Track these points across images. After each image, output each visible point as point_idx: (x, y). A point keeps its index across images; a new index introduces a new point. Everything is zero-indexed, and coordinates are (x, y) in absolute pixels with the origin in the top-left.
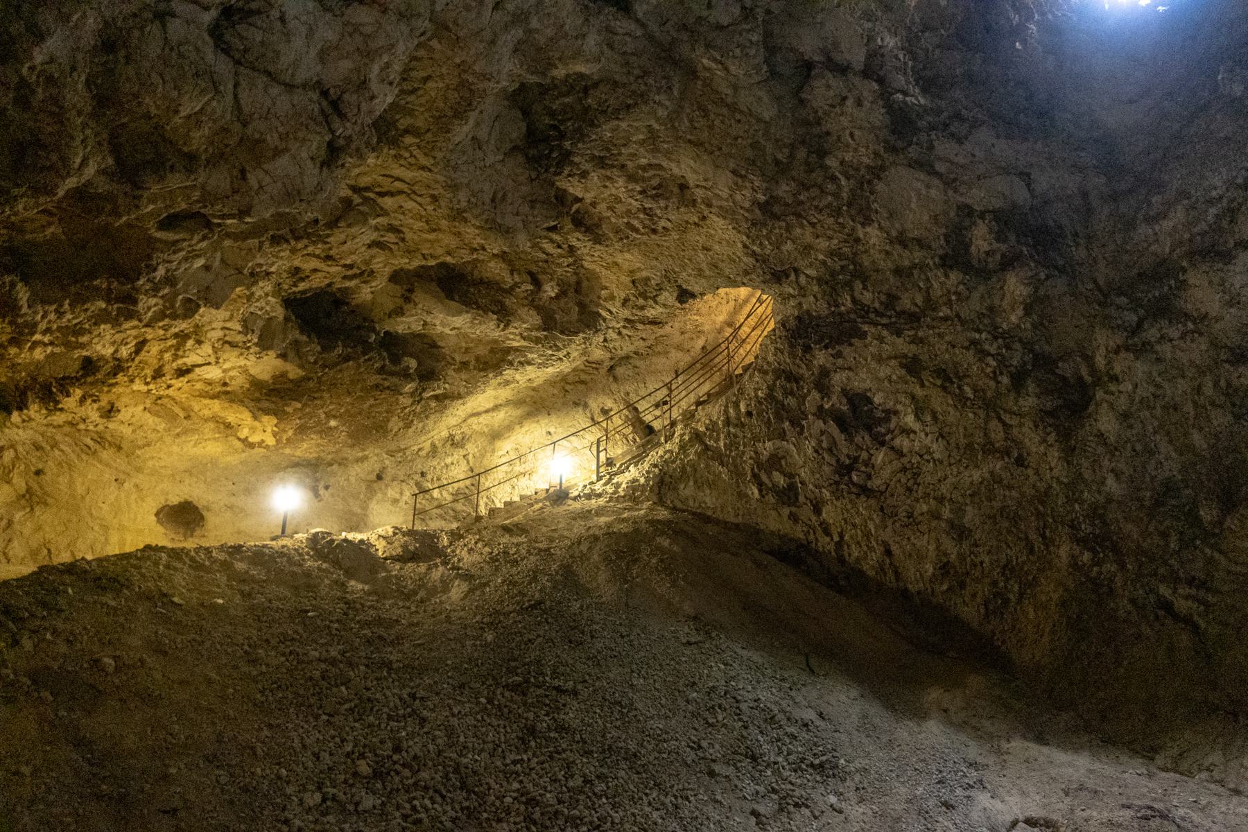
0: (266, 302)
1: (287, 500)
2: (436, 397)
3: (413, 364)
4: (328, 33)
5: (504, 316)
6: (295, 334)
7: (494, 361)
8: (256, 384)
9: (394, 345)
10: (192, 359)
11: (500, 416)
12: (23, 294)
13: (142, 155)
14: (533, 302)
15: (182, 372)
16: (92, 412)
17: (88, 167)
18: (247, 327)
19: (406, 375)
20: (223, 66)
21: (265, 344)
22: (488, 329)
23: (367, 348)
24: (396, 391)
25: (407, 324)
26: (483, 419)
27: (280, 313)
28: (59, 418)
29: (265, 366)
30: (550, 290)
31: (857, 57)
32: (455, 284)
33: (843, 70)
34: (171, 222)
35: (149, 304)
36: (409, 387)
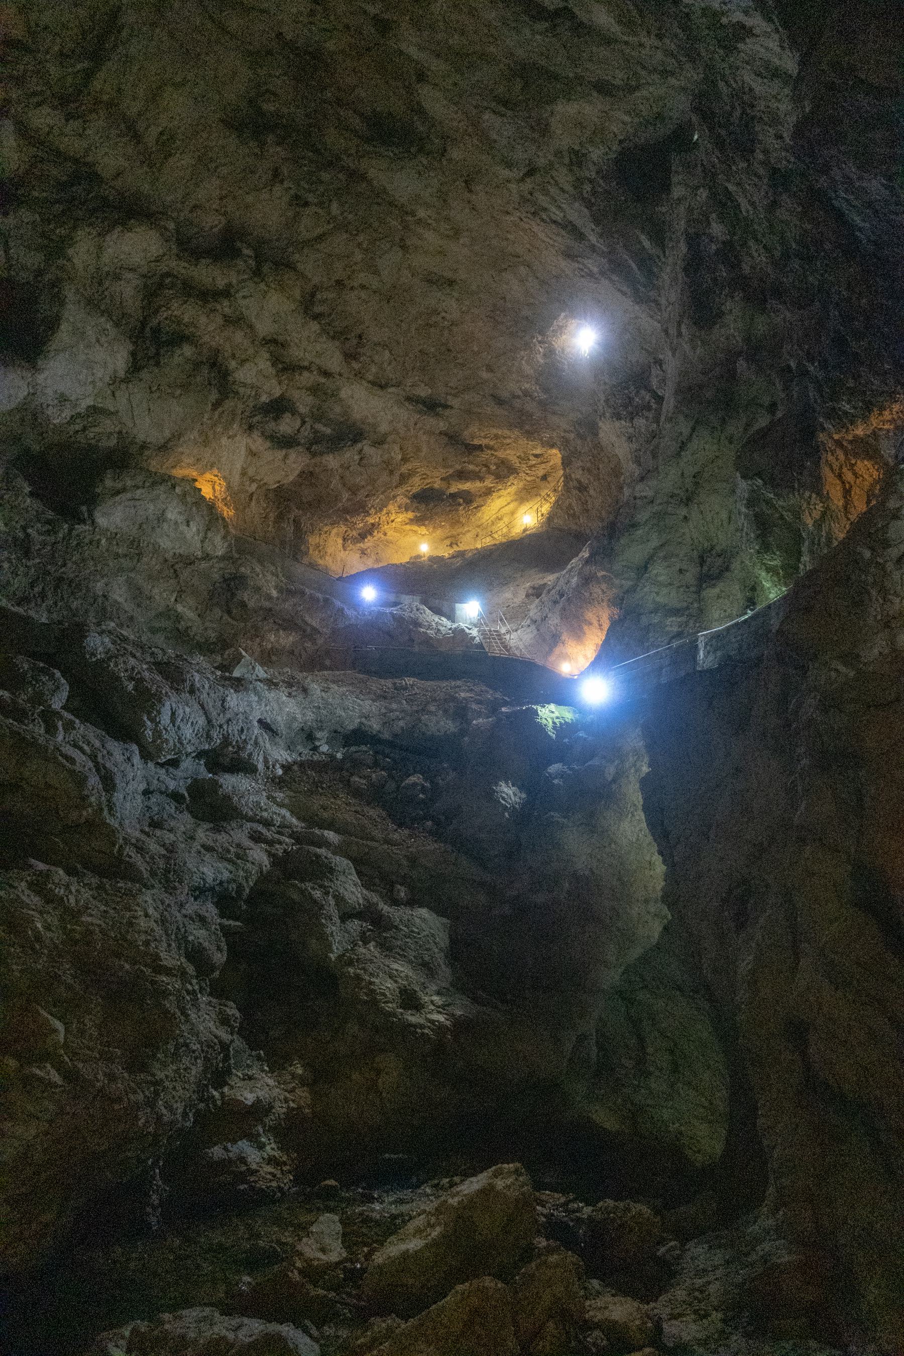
0: (402, 500)
1: (425, 548)
2: (475, 508)
3: (461, 501)
4: (380, 452)
5: (482, 479)
6: (415, 505)
7: (488, 492)
8: (411, 520)
9: (453, 496)
10: (392, 518)
11: (512, 506)
12: (348, 517)
13: (354, 490)
14: (489, 472)
15: (392, 521)
16: (381, 535)
17: (346, 495)
18: (399, 507)
19: (460, 505)
20: (362, 469)
21: (407, 510)
22: (478, 484)
23: (443, 500)
24: (457, 510)
25: (453, 489)
26: (506, 508)
27: (408, 501)
28: (375, 538)
29: (410, 515)
30: (493, 467)
31: (520, 394)
32: (462, 475)
33: (518, 397)
34: (367, 496)
35: (373, 511)
36: (461, 508)
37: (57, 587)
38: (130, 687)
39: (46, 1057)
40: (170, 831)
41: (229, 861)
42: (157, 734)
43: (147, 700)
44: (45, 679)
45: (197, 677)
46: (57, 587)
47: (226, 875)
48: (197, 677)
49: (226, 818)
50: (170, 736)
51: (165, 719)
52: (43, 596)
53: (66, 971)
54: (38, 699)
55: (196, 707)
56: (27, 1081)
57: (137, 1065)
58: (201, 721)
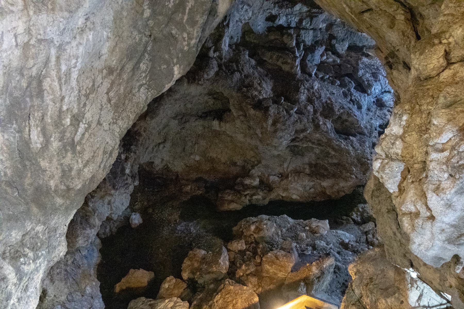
37: (351, 35)
38: (366, 83)
39: (354, 174)
40: (372, 111)
41: (382, 119)
42: (371, 92)
43: (370, 86)
44: (350, 84)
45: (381, 76)
46: (351, 35)
47: (381, 122)
48: (381, 76)
49: (383, 107)
50: (374, 93)
51: (373, 90)
52: (347, 37)
53: (356, 161)
54: (349, 90)
55: (379, 84)
56: (351, 177)
57: (364, 174)
58: (380, 88)
